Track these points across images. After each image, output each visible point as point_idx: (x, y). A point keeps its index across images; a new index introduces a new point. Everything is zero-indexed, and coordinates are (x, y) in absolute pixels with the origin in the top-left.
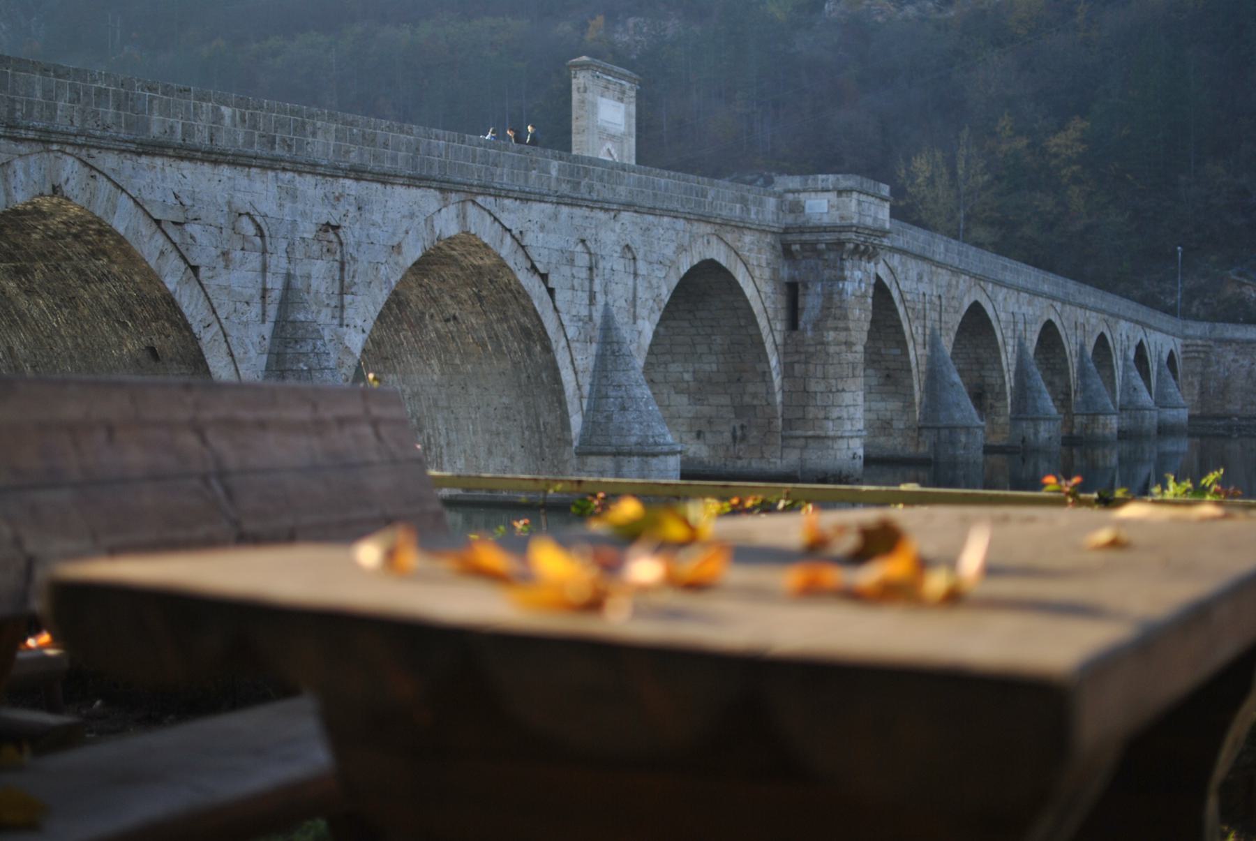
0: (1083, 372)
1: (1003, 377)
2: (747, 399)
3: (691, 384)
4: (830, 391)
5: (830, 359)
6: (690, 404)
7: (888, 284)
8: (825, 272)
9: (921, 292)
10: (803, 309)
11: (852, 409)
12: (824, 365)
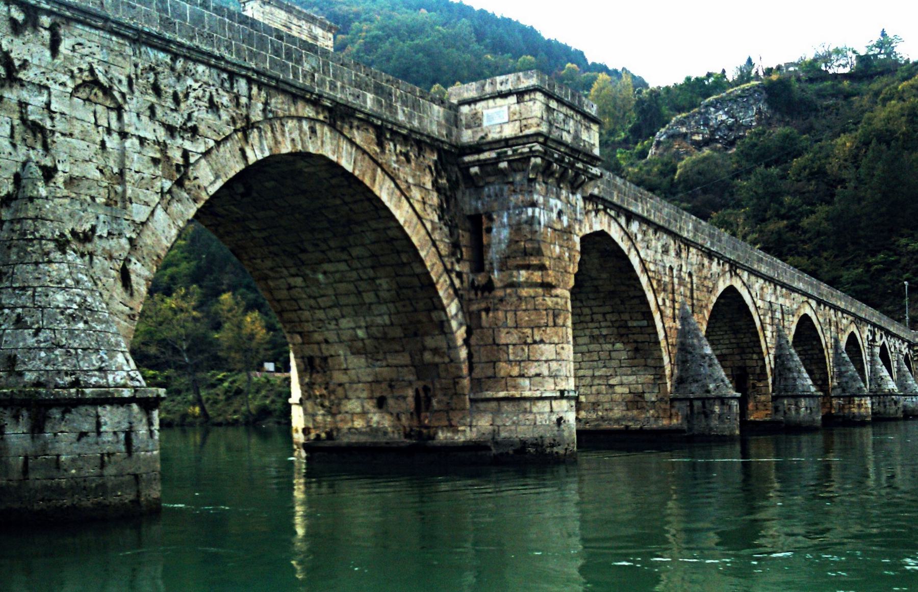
0: (838, 361)
1: (763, 359)
2: (428, 356)
3: (367, 342)
4: (525, 343)
5: (523, 304)
6: (368, 367)
7: (626, 252)
8: (512, 198)
9: (668, 265)
10: (489, 245)
11: (554, 365)
12: (515, 311)
